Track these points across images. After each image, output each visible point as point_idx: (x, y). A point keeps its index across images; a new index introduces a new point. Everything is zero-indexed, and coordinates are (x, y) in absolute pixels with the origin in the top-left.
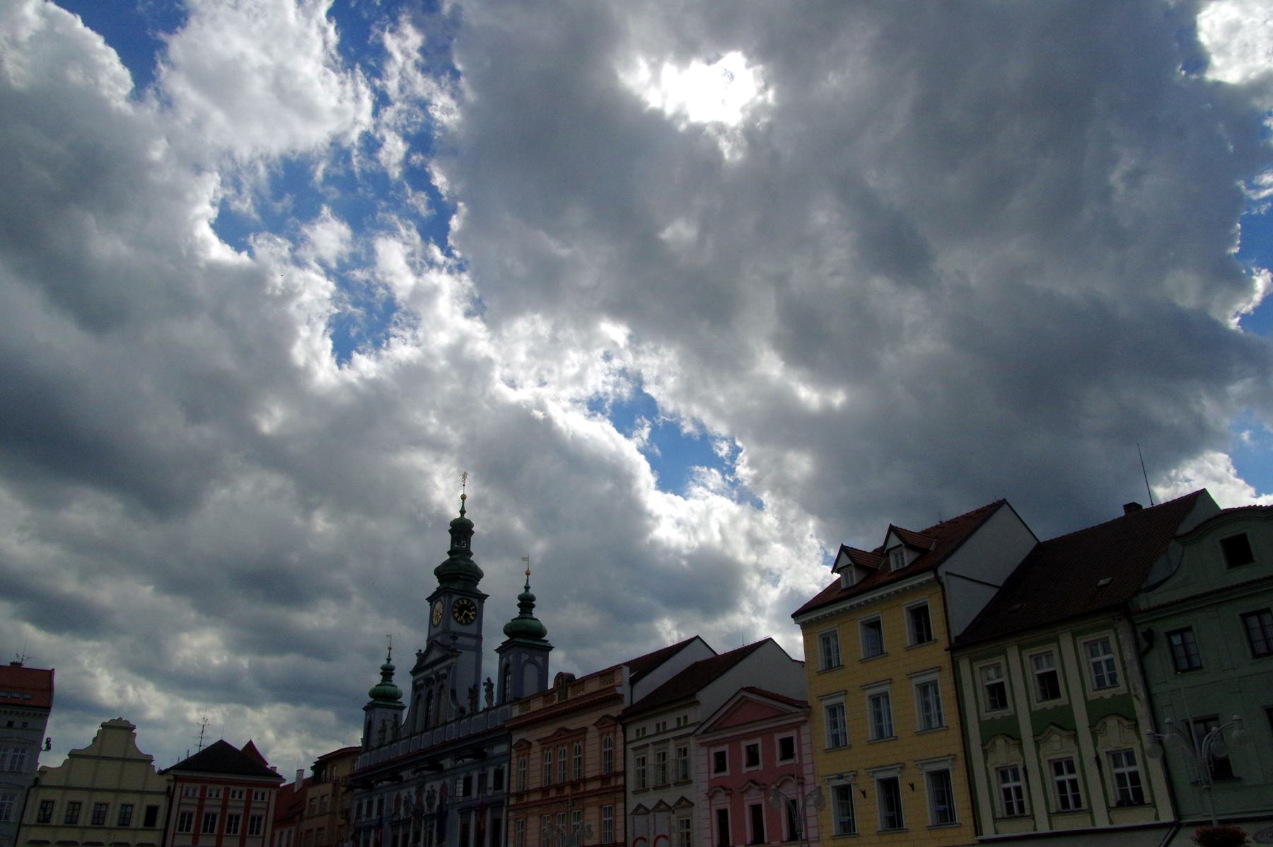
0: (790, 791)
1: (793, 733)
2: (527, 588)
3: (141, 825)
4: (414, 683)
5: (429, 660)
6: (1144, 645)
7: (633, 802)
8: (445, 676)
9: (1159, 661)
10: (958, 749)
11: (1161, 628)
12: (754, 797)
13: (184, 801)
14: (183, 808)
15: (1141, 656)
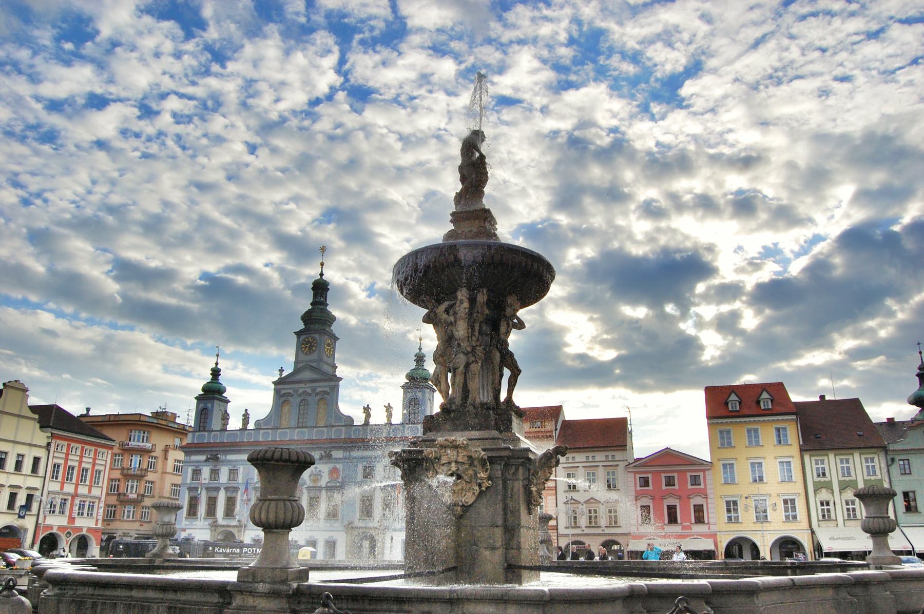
0: (698, 500)
1: (701, 474)
2: (420, 349)
3: (29, 472)
4: (277, 392)
5: (298, 377)
6: (890, 462)
7: (562, 497)
8: (328, 394)
9: (895, 470)
10: (801, 490)
11: (897, 458)
12: (672, 501)
13: (56, 455)
14: (56, 461)
15: (888, 466)
